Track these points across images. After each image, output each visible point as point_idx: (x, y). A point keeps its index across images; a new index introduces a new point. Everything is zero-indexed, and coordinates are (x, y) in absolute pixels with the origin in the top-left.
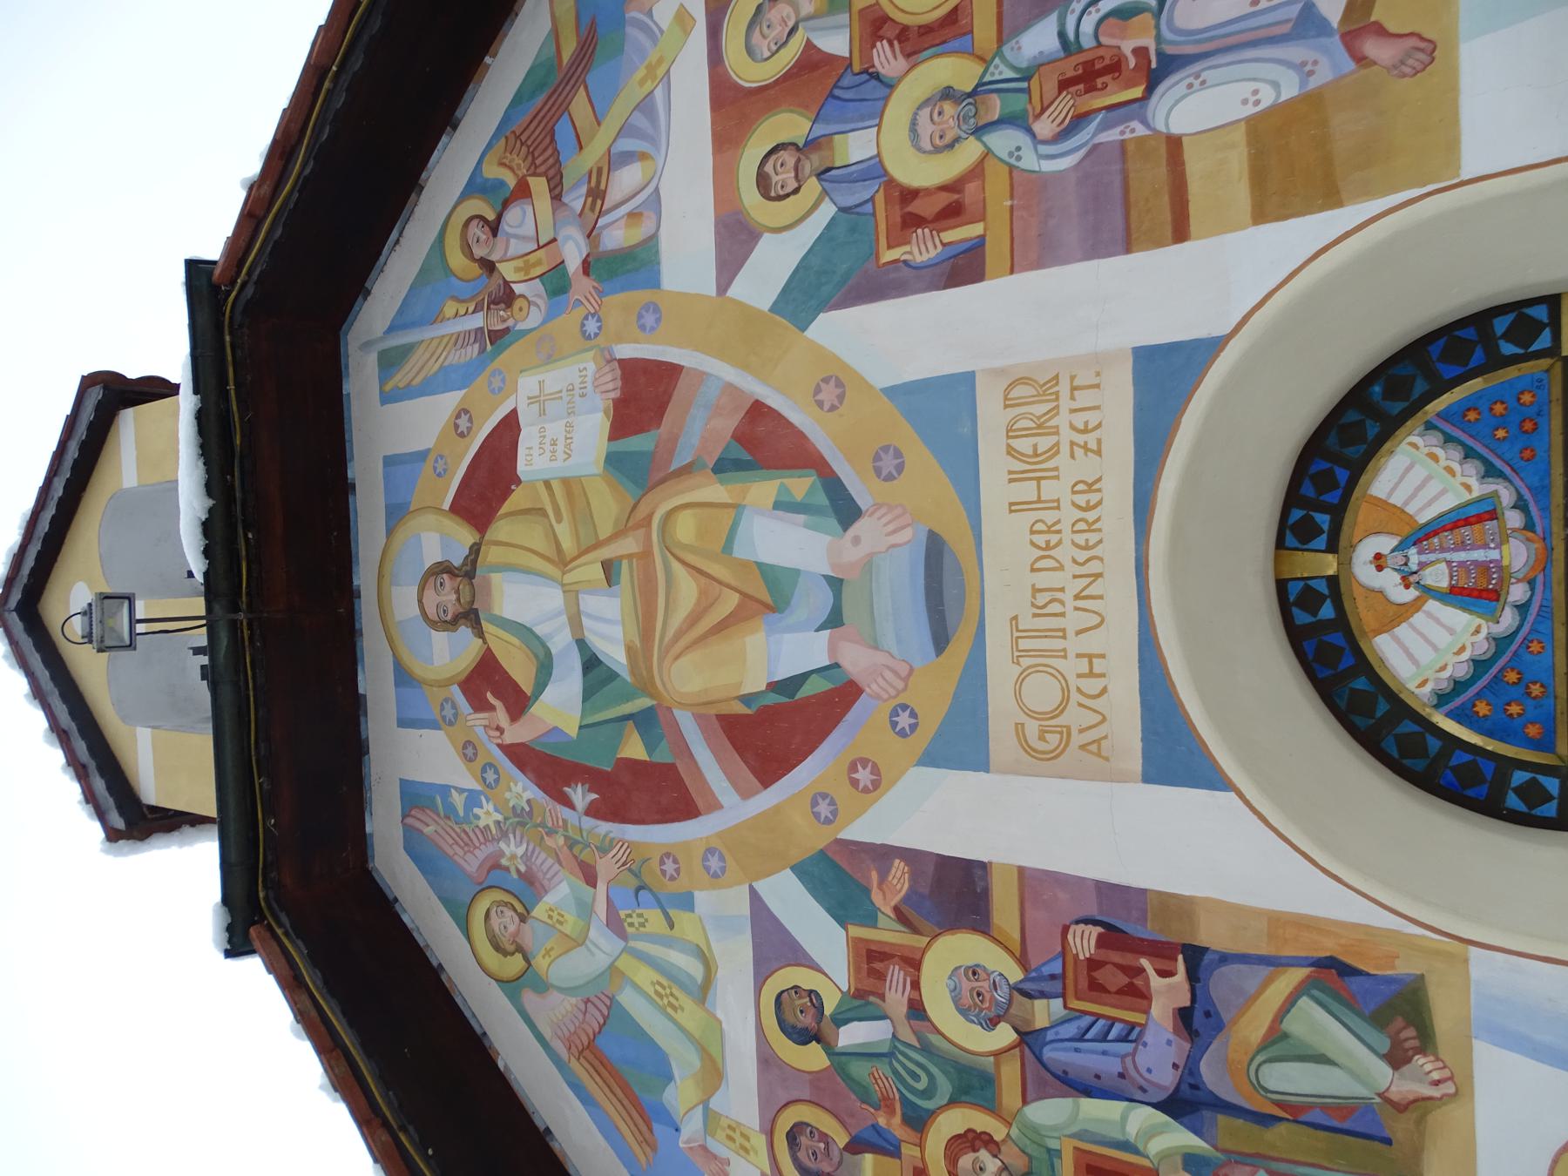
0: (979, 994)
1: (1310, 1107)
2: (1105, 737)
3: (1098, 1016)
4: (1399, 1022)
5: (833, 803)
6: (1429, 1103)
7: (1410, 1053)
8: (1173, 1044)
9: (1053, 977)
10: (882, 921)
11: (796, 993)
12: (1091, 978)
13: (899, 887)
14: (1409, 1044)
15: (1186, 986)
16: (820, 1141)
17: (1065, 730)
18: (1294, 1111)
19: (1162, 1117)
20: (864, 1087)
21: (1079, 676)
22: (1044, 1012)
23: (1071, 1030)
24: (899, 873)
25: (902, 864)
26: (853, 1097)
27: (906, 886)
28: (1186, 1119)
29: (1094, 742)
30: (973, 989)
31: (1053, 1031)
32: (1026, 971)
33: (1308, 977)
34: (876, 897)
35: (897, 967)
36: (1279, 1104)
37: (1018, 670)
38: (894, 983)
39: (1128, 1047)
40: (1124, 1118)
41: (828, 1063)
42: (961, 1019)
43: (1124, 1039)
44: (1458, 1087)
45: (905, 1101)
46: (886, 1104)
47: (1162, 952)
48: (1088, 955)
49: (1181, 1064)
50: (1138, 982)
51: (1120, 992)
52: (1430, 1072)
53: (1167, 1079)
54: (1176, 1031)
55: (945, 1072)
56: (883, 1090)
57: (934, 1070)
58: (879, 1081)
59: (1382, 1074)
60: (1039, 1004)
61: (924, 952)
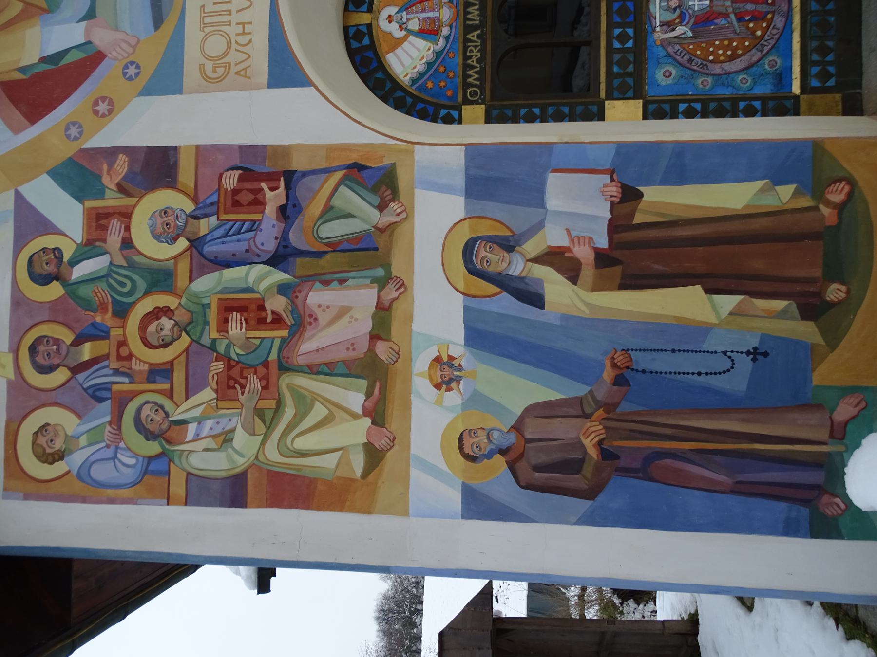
0: (167, 225)
1: (341, 242)
2: (250, 66)
3: (236, 221)
4: (384, 188)
5: (80, 127)
6: (396, 224)
7: (388, 202)
8: (276, 227)
9: (212, 204)
10: (108, 194)
11: (44, 252)
12: (234, 201)
13: (120, 171)
14: (387, 199)
15: (284, 193)
16: (53, 345)
17: (227, 65)
18: (334, 246)
19: (268, 268)
20: (88, 300)
21: (237, 35)
22: (205, 226)
23: (221, 232)
24: (121, 164)
25: (124, 156)
26: (80, 309)
27: (126, 169)
28: (280, 266)
29: (243, 69)
30: (164, 222)
31: (210, 235)
32: (197, 204)
33: (344, 175)
34: (106, 180)
35: (116, 220)
36: (327, 245)
37: (203, 34)
38: (113, 234)
39: (252, 234)
40: (247, 274)
41: (64, 292)
42: (156, 241)
43: (249, 230)
44: (407, 214)
45: (115, 302)
46: (103, 307)
47: (271, 178)
48: (232, 188)
49: (279, 237)
50: (259, 197)
51: (249, 204)
52: (396, 209)
53: (271, 246)
54: (278, 219)
55: (142, 277)
56: (101, 299)
57: (136, 277)
58: (99, 294)
59: (374, 215)
60: (203, 222)
61: (134, 207)
